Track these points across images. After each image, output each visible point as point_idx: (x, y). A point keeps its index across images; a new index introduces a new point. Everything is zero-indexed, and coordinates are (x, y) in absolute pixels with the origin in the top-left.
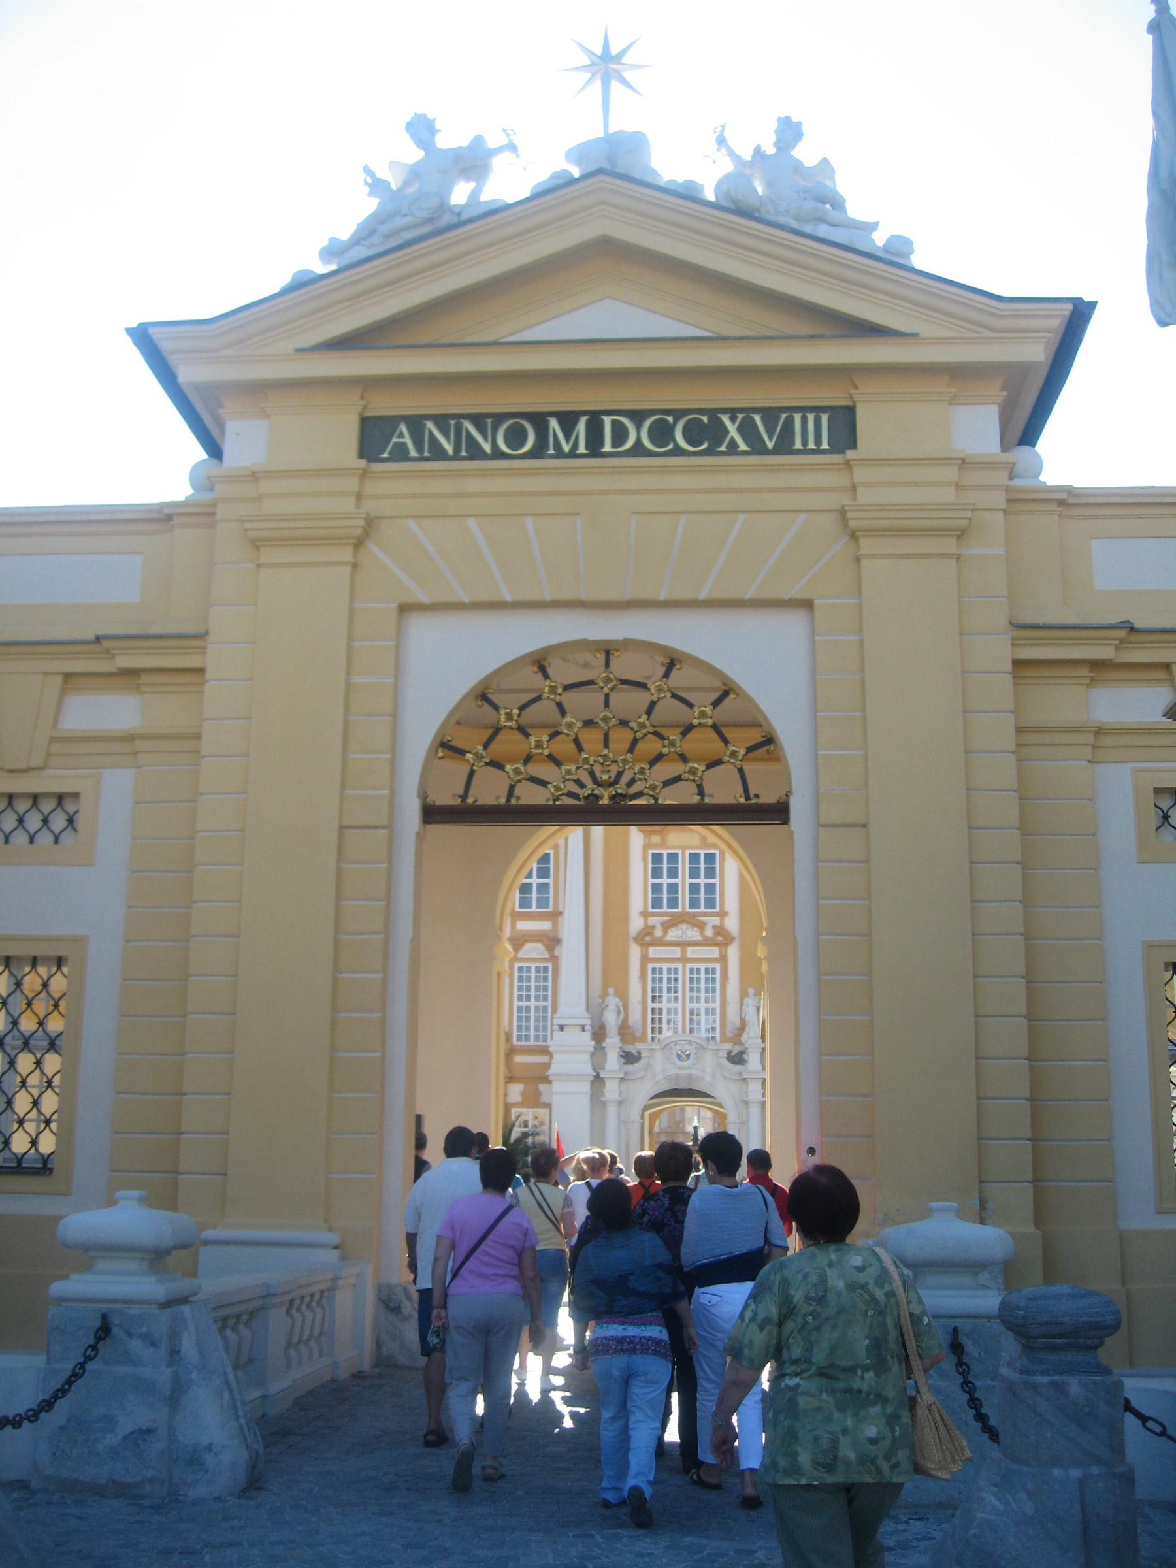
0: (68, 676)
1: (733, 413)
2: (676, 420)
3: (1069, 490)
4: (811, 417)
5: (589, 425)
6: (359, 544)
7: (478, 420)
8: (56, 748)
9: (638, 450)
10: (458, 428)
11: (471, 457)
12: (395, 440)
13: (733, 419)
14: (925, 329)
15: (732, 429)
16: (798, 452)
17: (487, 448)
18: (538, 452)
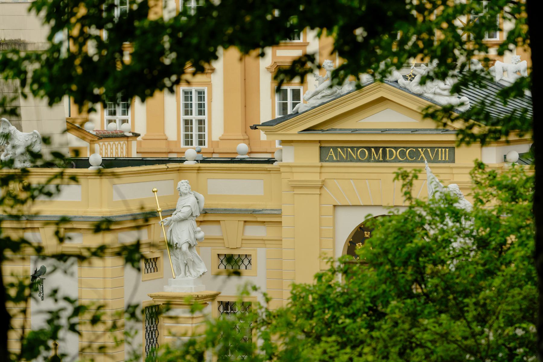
0: (245, 222)
1: (422, 148)
2: (406, 151)
5: (382, 150)
6: (321, 188)
7: (352, 148)
8: (244, 242)
10: (347, 150)
11: (351, 161)
12: (329, 154)
13: (422, 150)
15: (422, 153)
16: (440, 162)
17: (355, 157)
18: (368, 160)
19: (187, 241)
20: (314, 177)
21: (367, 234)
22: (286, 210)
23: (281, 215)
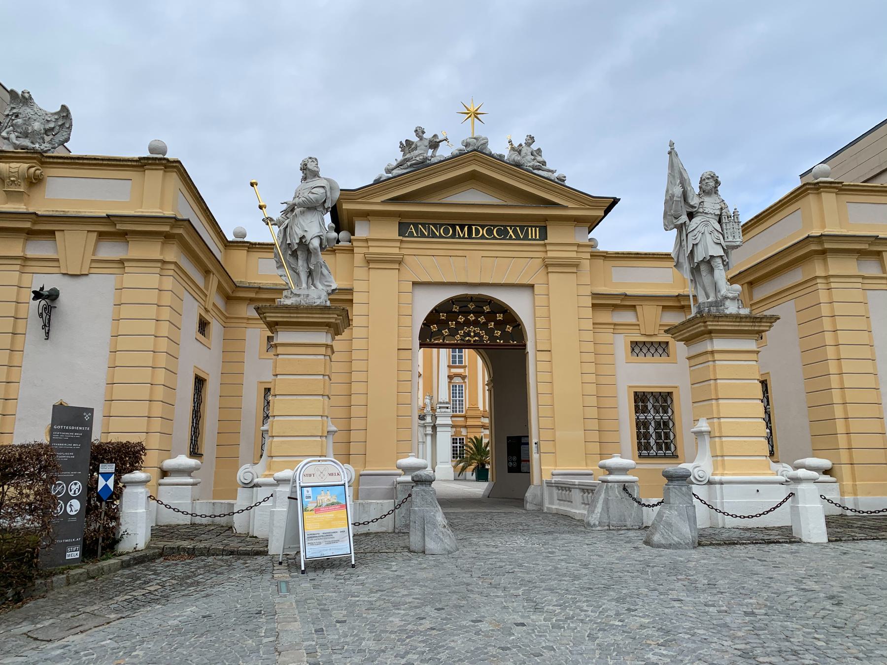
3: (607, 252)
4: (534, 229)
6: (400, 263)
9: (483, 237)
10: (429, 227)
13: (511, 229)
14: (570, 205)
16: (530, 240)
17: (438, 234)
18: (452, 237)
19: (319, 234)
20: (393, 250)
21: (443, 316)
22: (357, 286)
23: (351, 292)
